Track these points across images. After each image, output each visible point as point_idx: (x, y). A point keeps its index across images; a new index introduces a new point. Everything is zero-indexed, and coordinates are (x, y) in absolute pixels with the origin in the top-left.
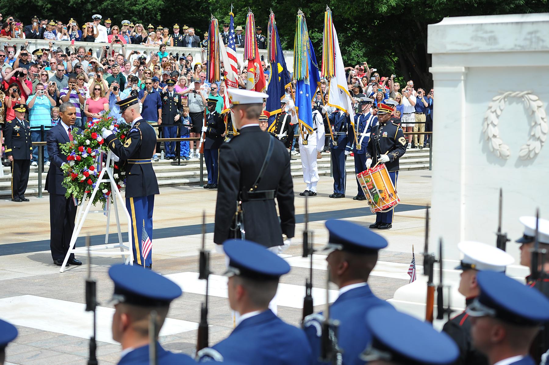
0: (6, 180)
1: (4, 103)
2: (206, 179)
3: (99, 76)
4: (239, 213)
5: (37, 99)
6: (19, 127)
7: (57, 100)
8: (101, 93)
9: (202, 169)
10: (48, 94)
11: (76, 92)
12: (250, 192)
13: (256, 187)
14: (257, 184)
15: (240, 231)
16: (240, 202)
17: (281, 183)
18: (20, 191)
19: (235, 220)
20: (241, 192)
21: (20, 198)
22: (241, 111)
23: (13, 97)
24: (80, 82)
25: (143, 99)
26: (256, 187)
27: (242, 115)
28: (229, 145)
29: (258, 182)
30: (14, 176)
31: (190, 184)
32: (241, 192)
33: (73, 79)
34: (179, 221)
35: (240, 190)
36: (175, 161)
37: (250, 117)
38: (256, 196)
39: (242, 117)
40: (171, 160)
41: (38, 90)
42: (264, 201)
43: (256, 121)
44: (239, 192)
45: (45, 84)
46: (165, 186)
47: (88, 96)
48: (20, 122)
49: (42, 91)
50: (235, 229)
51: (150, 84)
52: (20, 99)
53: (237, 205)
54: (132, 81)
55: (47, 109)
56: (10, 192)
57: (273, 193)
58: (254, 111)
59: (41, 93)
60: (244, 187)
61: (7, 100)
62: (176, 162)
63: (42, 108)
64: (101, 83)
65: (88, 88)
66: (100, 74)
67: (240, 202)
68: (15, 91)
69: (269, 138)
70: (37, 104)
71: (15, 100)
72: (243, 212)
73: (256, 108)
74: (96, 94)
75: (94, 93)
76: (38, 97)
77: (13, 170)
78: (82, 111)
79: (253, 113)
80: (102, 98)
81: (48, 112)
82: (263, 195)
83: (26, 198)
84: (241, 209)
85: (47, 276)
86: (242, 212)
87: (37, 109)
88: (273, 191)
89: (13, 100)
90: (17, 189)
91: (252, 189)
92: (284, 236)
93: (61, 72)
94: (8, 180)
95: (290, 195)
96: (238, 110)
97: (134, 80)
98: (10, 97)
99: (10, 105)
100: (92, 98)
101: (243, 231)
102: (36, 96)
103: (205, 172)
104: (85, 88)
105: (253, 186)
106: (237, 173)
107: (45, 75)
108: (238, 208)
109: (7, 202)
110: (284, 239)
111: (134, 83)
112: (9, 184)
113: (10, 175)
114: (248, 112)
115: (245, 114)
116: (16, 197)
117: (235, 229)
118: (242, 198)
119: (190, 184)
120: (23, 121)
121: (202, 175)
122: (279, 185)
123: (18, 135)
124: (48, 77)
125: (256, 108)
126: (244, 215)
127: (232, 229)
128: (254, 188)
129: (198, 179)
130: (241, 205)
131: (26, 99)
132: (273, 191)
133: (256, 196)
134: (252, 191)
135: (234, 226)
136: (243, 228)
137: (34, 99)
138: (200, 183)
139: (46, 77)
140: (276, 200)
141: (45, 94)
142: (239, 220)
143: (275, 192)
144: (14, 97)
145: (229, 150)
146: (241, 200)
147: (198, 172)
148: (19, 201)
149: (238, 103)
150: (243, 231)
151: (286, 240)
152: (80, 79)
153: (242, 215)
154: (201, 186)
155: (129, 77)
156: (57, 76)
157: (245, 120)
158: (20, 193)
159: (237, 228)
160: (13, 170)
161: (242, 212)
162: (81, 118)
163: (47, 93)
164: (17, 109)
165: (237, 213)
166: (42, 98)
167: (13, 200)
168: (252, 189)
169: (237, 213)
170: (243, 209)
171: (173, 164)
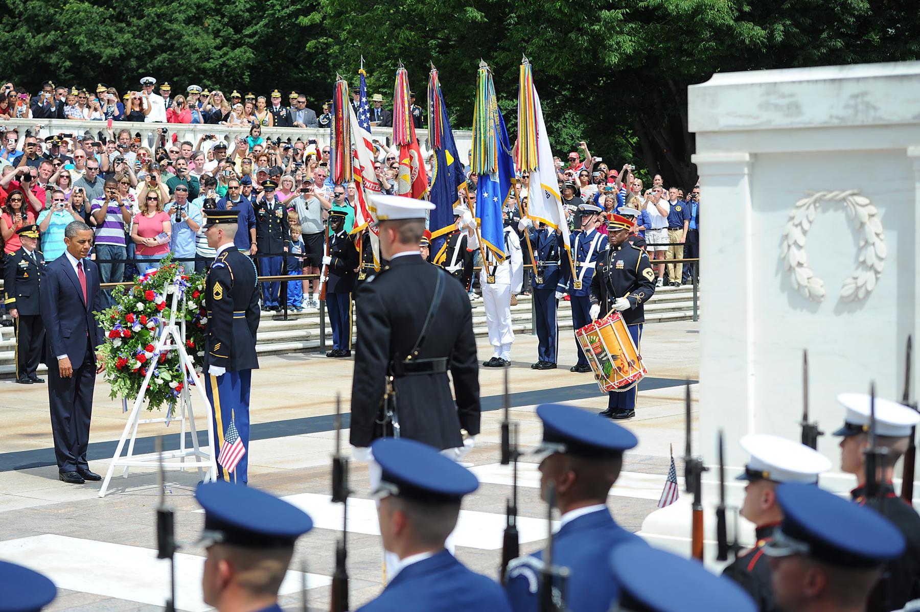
0: (6, 349)
2: (329, 342)
3: (154, 178)
4: (390, 396)
5: (53, 215)
6: (28, 262)
7: (87, 216)
8: (157, 206)
9: (322, 325)
11: (118, 204)
12: (407, 361)
13: (416, 353)
14: (418, 349)
15: (392, 426)
16: (392, 378)
17: (457, 346)
18: (29, 366)
19: (383, 407)
20: (392, 362)
21: (29, 377)
22: (391, 232)
24: (123, 188)
26: (416, 353)
27: (392, 237)
28: (372, 287)
29: (420, 346)
30: (19, 341)
31: (305, 350)
32: (392, 362)
33: (111, 183)
34: (288, 411)
35: (391, 359)
36: (279, 314)
37: (405, 241)
38: (416, 367)
39: (393, 241)
40: (273, 313)
42: (430, 375)
43: (415, 247)
44: (389, 363)
45: (67, 192)
46: (263, 354)
47: (136, 210)
48: (29, 253)
50: (384, 422)
51: (236, 188)
53: (387, 382)
54: (206, 185)
56: (13, 368)
57: (445, 363)
58: (411, 230)
59: (59, 207)
60: (397, 354)
62: (281, 315)
64: (157, 188)
65: (136, 197)
66: (155, 174)
67: (392, 378)
69: (435, 275)
70: (54, 225)
72: (396, 394)
73: (414, 225)
75: (147, 205)
76: (56, 213)
77: (17, 332)
78: (127, 234)
79: (409, 234)
80: (159, 213)
82: (429, 366)
83: (39, 377)
84: (394, 390)
85: (79, 503)
86: (394, 393)
88: (445, 359)
90: (24, 363)
91: (410, 357)
92: (464, 432)
93: (93, 171)
94: (9, 349)
95: (473, 366)
96: (386, 230)
97: (210, 182)
100: (143, 214)
101: (396, 425)
102: (52, 212)
103: (329, 330)
104: (131, 197)
105: (412, 351)
106: (386, 331)
108: (389, 388)
109: (10, 384)
110: (464, 438)
112: (11, 355)
113: (13, 341)
114: (402, 233)
115: (398, 236)
116: (23, 376)
117: (384, 422)
118: (394, 372)
119: (305, 350)
120: (33, 252)
121: (323, 336)
122: (453, 350)
123: (26, 275)
125: (414, 225)
126: (397, 399)
127: (378, 422)
128: (413, 355)
129: (317, 342)
130: (392, 382)
131: (36, 217)
132: (445, 359)
133: (416, 367)
134: (410, 359)
135: (382, 417)
136: (397, 419)
137: (49, 217)
138: (321, 349)
140: (449, 373)
141: (67, 209)
142: (390, 406)
143: (448, 361)
145: (371, 295)
146: (392, 374)
147: (317, 331)
148: (27, 382)
149: (386, 218)
150: (396, 425)
151: (467, 438)
152: (122, 183)
153: (394, 399)
154: (322, 352)
156: (87, 178)
157: (397, 245)
158: (29, 369)
159: (387, 419)
160: (17, 332)
161: (394, 393)
162: (125, 246)
163: (69, 207)
165: (386, 396)
166: (61, 214)
167: (17, 382)
168: (410, 357)
169: (386, 396)
170: (396, 389)
171: (275, 318)
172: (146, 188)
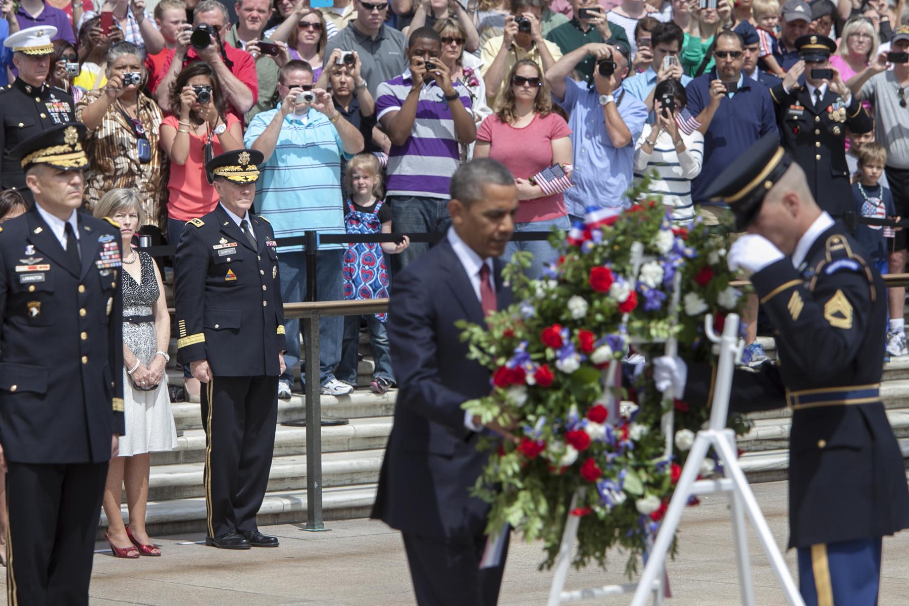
1: (161, 147)
3: (525, 26)
5: (285, 124)
7: (366, 124)
8: (538, 99)
10: (331, 103)
11: (442, 94)
23: (196, 118)
25: (707, 116)
41: (293, 90)
45: (315, 63)
47: (481, 110)
49: (308, 93)
51: (735, 54)
52: (221, 128)
54: (654, 43)
55: (328, 165)
59: (302, 102)
61: (171, 131)
63: (307, 160)
64: (532, 52)
65: (479, 75)
66: (529, 15)
68: (206, 96)
70: (289, 146)
71: (202, 130)
74: (522, 101)
75: (511, 97)
76: (290, 117)
80: (542, 117)
81: (329, 176)
87: (287, 168)
89: (193, 133)
93: (376, 11)
97: (664, 35)
98: (186, 121)
99: (182, 152)
100: (501, 117)
102: (284, 113)
104: (469, 74)
107: (311, 28)
111: (664, 52)
124: (323, 36)
131: (244, 125)
137: (274, 126)
139: (316, 35)
141: (321, 105)
144: (200, 122)
155: (642, 26)
156: (359, 28)
163: (325, 102)
164: (224, 171)
166: (305, 120)
172: (506, 51)
